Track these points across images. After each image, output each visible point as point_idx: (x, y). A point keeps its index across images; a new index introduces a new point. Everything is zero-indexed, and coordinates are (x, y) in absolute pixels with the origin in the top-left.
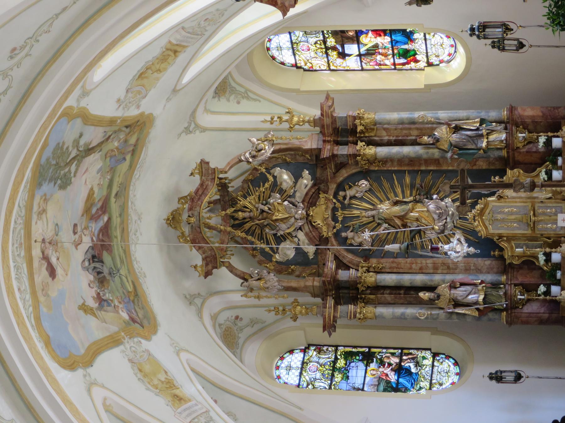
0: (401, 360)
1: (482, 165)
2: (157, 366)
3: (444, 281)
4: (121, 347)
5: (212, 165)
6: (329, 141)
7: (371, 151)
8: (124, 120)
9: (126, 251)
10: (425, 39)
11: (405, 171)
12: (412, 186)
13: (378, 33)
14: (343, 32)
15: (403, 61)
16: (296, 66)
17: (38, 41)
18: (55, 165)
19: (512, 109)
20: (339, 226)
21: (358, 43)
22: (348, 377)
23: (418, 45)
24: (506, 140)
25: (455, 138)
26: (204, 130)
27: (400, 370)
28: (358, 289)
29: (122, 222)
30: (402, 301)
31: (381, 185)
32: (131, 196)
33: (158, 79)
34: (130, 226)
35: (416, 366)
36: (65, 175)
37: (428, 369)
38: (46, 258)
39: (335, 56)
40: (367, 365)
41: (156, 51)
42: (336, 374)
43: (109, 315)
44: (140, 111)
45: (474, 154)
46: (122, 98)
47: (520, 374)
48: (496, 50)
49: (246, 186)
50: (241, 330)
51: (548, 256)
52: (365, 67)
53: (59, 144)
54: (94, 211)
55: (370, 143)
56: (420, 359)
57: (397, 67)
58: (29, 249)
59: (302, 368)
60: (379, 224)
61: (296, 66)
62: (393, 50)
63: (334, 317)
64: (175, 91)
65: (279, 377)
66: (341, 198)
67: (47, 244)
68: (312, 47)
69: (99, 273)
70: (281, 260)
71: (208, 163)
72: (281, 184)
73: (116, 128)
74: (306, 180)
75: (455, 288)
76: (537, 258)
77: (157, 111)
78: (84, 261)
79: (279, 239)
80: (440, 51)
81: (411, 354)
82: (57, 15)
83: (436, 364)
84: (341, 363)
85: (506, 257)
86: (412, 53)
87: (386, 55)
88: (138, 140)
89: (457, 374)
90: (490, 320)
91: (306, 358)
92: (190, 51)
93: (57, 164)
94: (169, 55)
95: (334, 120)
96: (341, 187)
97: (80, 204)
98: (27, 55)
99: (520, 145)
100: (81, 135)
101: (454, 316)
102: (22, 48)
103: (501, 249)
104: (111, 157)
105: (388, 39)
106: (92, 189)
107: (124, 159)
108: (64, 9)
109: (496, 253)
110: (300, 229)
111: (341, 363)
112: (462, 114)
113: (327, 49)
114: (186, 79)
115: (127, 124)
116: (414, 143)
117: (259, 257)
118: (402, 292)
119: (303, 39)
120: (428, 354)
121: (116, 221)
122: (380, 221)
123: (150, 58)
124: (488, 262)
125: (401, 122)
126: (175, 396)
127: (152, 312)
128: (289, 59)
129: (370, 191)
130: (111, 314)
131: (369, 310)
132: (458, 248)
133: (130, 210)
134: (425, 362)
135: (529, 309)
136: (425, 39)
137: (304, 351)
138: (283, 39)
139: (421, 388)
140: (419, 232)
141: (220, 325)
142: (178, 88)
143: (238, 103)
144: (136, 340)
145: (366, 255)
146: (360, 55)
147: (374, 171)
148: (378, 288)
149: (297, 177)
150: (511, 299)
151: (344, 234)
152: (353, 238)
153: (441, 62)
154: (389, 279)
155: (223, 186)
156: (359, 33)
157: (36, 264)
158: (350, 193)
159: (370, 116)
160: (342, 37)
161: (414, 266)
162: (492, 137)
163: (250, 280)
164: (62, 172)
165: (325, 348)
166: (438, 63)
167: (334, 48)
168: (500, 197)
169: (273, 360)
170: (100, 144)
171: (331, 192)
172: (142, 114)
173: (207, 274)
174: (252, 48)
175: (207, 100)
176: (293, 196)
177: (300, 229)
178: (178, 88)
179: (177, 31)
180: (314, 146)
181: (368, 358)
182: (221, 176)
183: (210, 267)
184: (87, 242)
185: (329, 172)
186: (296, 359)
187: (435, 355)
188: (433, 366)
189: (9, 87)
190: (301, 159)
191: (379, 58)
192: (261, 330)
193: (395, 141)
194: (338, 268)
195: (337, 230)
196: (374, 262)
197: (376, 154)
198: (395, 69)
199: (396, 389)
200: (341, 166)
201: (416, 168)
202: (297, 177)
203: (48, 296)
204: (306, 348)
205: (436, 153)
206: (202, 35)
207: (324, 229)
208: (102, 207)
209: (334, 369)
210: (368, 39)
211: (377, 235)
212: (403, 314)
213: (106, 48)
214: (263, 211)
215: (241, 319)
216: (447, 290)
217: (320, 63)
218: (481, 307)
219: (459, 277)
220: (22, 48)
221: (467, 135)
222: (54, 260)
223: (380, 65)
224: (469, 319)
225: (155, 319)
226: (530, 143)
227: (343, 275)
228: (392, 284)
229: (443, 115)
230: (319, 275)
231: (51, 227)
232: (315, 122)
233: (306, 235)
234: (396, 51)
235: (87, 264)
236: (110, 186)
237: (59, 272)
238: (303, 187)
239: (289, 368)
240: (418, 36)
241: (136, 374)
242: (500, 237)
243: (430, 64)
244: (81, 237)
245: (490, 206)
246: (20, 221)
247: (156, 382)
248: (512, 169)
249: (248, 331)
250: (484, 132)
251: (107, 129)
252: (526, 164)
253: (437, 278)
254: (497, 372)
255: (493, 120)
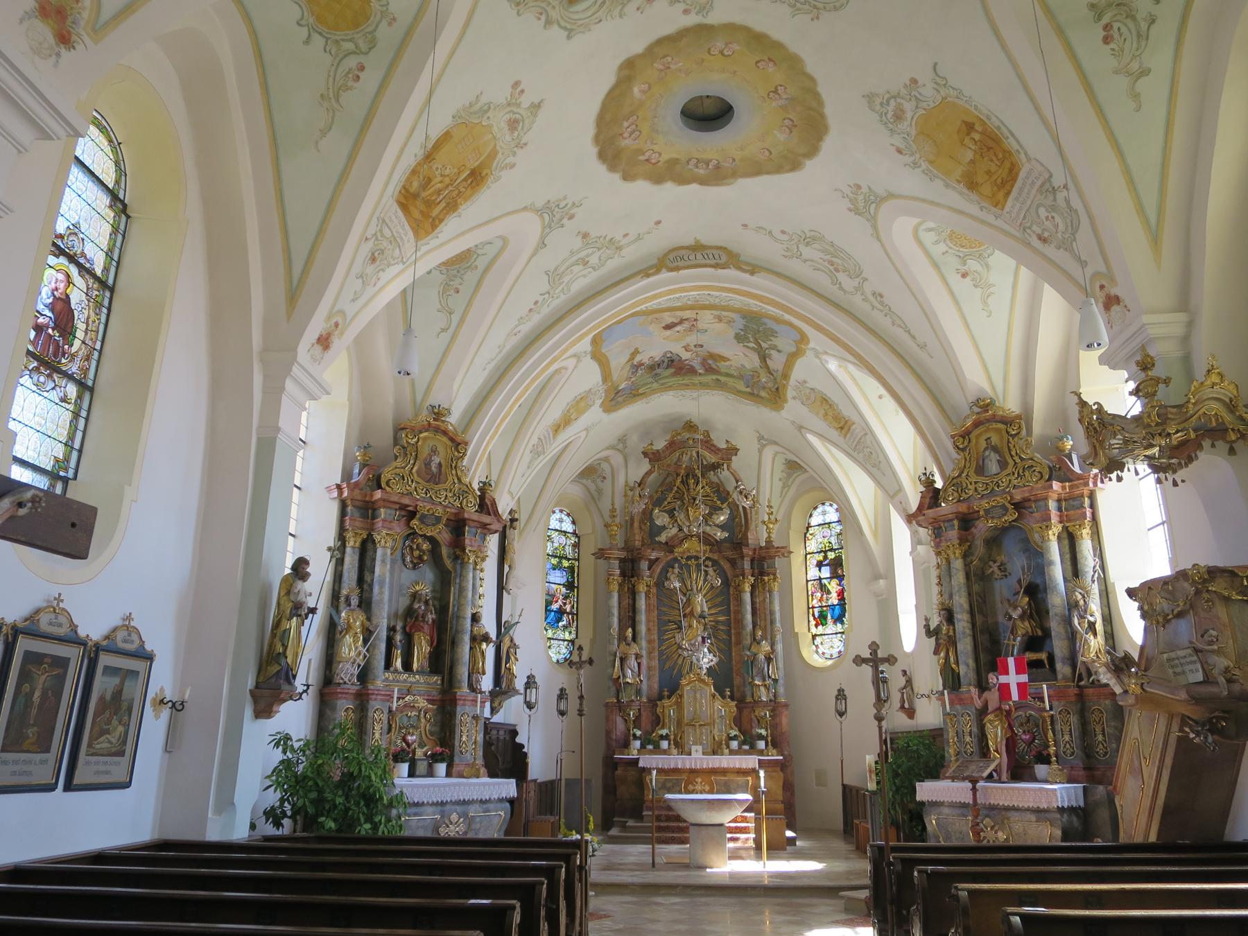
0: (568, 614)
1: (737, 681)
2: (581, 413)
3: (641, 649)
4: (601, 383)
5: (734, 458)
6: (755, 553)
7: (747, 588)
8: (785, 386)
9: (670, 388)
10: (836, 633)
11: (730, 616)
12: (717, 622)
13: (841, 594)
14: (841, 565)
15: (817, 615)
16: (809, 526)
17: (886, 316)
18: (758, 330)
19: (786, 706)
20: (684, 561)
21: (831, 578)
22: (554, 569)
23: (831, 627)
24: (762, 701)
25: (761, 657)
26: (760, 451)
27: (561, 612)
28: (633, 577)
29: (694, 385)
30: (622, 613)
31: (717, 596)
32: (714, 392)
33: (817, 414)
34: (689, 391)
35: (564, 626)
36: (748, 338)
37: (562, 636)
38: (681, 322)
39: (818, 559)
40: (564, 585)
41: (847, 412)
42: (557, 559)
43: (625, 373)
44: (789, 399)
45: (748, 673)
46: (807, 385)
47: (843, 714)
48: (836, 693)
49: (714, 485)
50: (593, 482)
51: (666, 737)
52: (810, 583)
53: (777, 333)
54: (710, 362)
55: (753, 586)
56: (569, 629)
57: (811, 610)
58: (692, 308)
59: (561, 531)
60: (685, 595)
61: (809, 526)
62: (826, 606)
63: (610, 558)
64: (800, 428)
65: (554, 512)
66: (707, 563)
67: (692, 323)
68: (826, 539)
69: (659, 365)
70: (654, 514)
71: (736, 455)
72: (716, 514)
73: (778, 380)
74: (720, 535)
75: (636, 659)
76: (663, 728)
77: (784, 413)
78: (671, 353)
79: (671, 513)
80: (826, 646)
81: (573, 622)
82: (909, 332)
83: (566, 643)
84: (566, 563)
85: (663, 701)
86: (824, 622)
87: (821, 600)
88: (763, 398)
89: (558, 661)
90: (609, 688)
91: (569, 535)
92: (841, 441)
93: (759, 331)
94: (839, 423)
95: (773, 558)
96: (715, 563)
97: (716, 350)
98: (873, 307)
99: (757, 713)
100: (779, 351)
101: (612, 658)
102: (882, 303)
103: (669, 697)
104: (753, 376)
105: (836, 602)
106: (729, 360)
107: (748, 387)
108: (913, 337)
109: (666, 693)
110: (681, 530)
111: (566, 563)
112: (781, 665)
113: (825, 552)
114: (810, 437)
115: (780, 389)
116: (755, 625)
117: (656, 497)
118: (630, 614)
119: (833, 533)
120: (573, 636)
121: (696, 379)
122: (688, 596)
123: (840, 408)
124: (656, 686)
125: (772, 613)
126: (559, 426)
127: (619, 409)
128: (815, 520)
129: (712, 587)
130: (626, 375)
131: (615, 587)
132: (706, 660)
133: (702, 391)
134: (567, 633)
135: (619, 721)
136: (836, 633)
137: (574, 533)
138: (832, 516)
139: (547, 630)
140: (680, 628)
141: (600, 464)
142: (803, 430)
143: (780, 480)
144: (603, 395)
145: (660, 584)
146: (820, 579)
147: (729, 591)
148: (633, 594)
149: (723, 527)
150: (628, 706)
151: (677, 565)
152: (673, 573)
153: (817, 646)
154: (642, 603)
155: (715, 467)
156: (841, 578)
157: (679, 313)
158: (710, 570)
159: (776, 587)
160: (836, 564)
161: (652, 624)
162: (762, 689)
163: (640, 489)
164: (750, 336)
165: (577, 550)
166: (816, 643)
167: (825, 557)
168: (714, 696)
169: (566, 508)
170: (768, 367)
171: (711, 555)
172: (786, 401)
173: (645, 454)
174: (831, 492)
175: (785, 454)
176: (707, 524)
177: (681, 530)
178: (803, 430)
179: (864, 429)
180: (750, 541)
181: (570, 586)
182: (725, 465)
183: (651, 456)
184: (685, 355)
185: (729, 553)
186: (568, 527)
187: (572, 642)
188: (564, 640)
189: (845, 292)
190: (737, 530)
191: (819, 595)
192: (593, 498)
193: (756, 608)
194: (650, 560)
195: (679, 560)
196: (654, 590)
197: (746, 592)
198: (809, 608)
199: (548, 611)
200: (733, 563)
201: (732, 625)
202: (723, 527)
203: (651, 323)
204: (577, 535)
205: (748, 641)
206: (855, 450)
207: (681, 550)
208: (711, 368)
209: (561, 558)
210: (835, 586)
211: (677, 594)
212: (613, 615)
213: (877, 372)
214: (694, 499)
215: (603, 481)
216: (634, 651)
217: (812, 546)
218: (621, 680)
219: (644, 661)
220: (882, 303)
221: (764, 668)
222: (678, 328)
223: (812, 596)
224: (610, 670)
225: (614, 411)
226: (759, 721)
227: (644, 565)
228: (637, 606)
229: (779, 647)
230: (642, 545)
231: (705, 326)
232: (769, 542)
233: (676, 535)
234: (825, 609)
235: (668, 355)
236: (728, 375)
237: (668, 333)
238: (714, 532)
239: (561, 521)
240: (839, 628)
241: (580, 395)
242: (681, 696)
243: (814, 637)
244: (692, 350)
245: (706, 688)
246: (717, 300)
247: (571, 411)
248: (736, 705)
249: (592, 487)
250: (767, 682)
251: (780, 373)
252: (740, 718)
253: (644, 643)
254: (567, 694)
255: (777, 690)
